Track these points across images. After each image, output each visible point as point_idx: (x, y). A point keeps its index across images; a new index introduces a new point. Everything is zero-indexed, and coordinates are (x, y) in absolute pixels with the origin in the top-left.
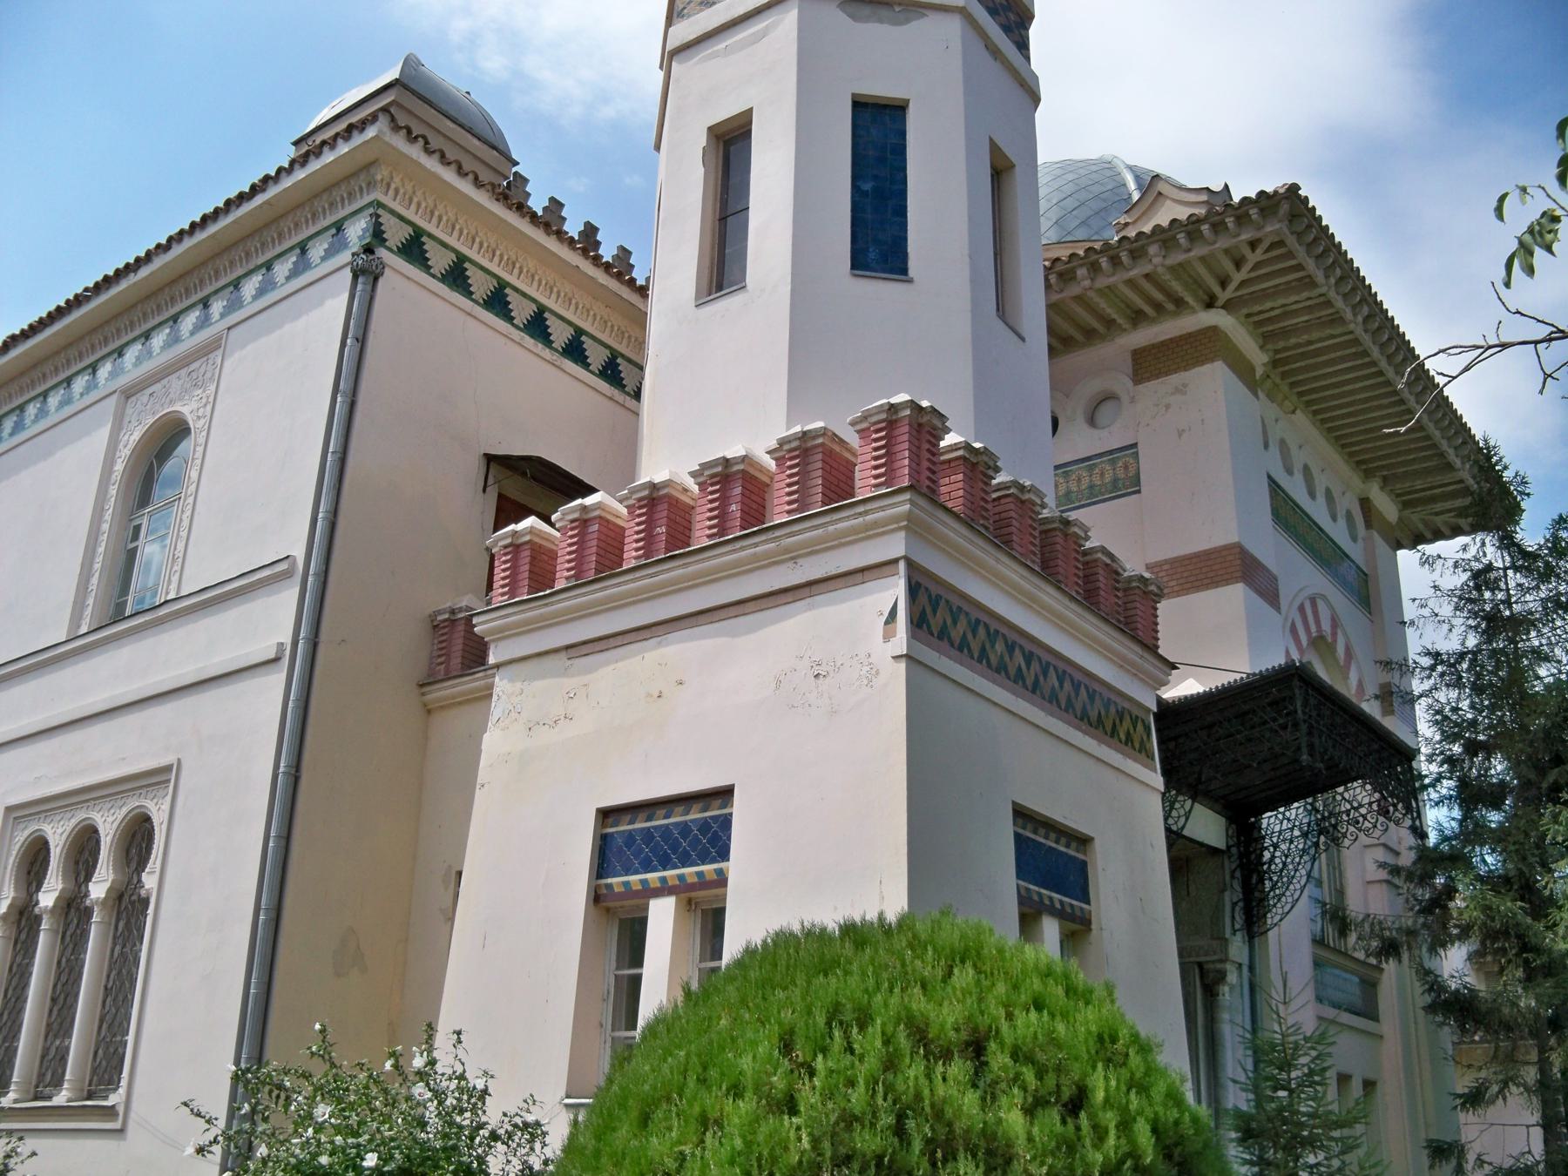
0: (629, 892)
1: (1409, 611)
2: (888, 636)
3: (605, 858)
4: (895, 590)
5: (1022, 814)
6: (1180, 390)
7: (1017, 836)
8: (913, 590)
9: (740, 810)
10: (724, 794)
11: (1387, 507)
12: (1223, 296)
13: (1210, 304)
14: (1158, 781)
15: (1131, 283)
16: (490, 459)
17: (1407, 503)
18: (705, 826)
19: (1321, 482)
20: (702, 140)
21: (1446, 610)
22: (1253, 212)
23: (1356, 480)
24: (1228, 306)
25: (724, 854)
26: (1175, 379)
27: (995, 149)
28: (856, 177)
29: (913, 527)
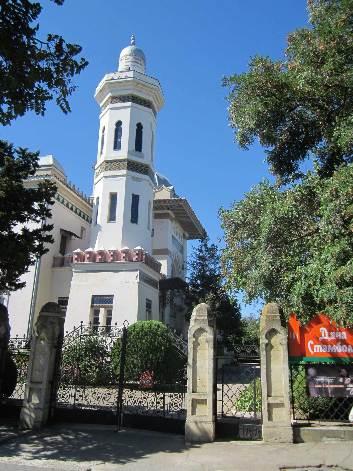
0: (97, 307)
1: (188, 254)
2: (136, 279)
3: (93, 302)
4: (137, 273)
5: (147, 299)
6: (162, 222)
7: (146, 302)
8: (140, 273)
9: (114, 298)
10: (112, 296)
11: (187, 235)
12: (170, 208)
13: (168, 209)
14: (158, 291)
15: (158, 206)
16: (61, 229)
17: (190, 234)
18: (109, 299)
19: (179, 232)
20: (109, 195)
21: (194, 256)
22: (179, 201)
23: (183, 231)
24: (171, 210)
25: (112, 303)
26: (161, 220)
27: (149, 201)
28: (132, 207)
29: (140, 266)
